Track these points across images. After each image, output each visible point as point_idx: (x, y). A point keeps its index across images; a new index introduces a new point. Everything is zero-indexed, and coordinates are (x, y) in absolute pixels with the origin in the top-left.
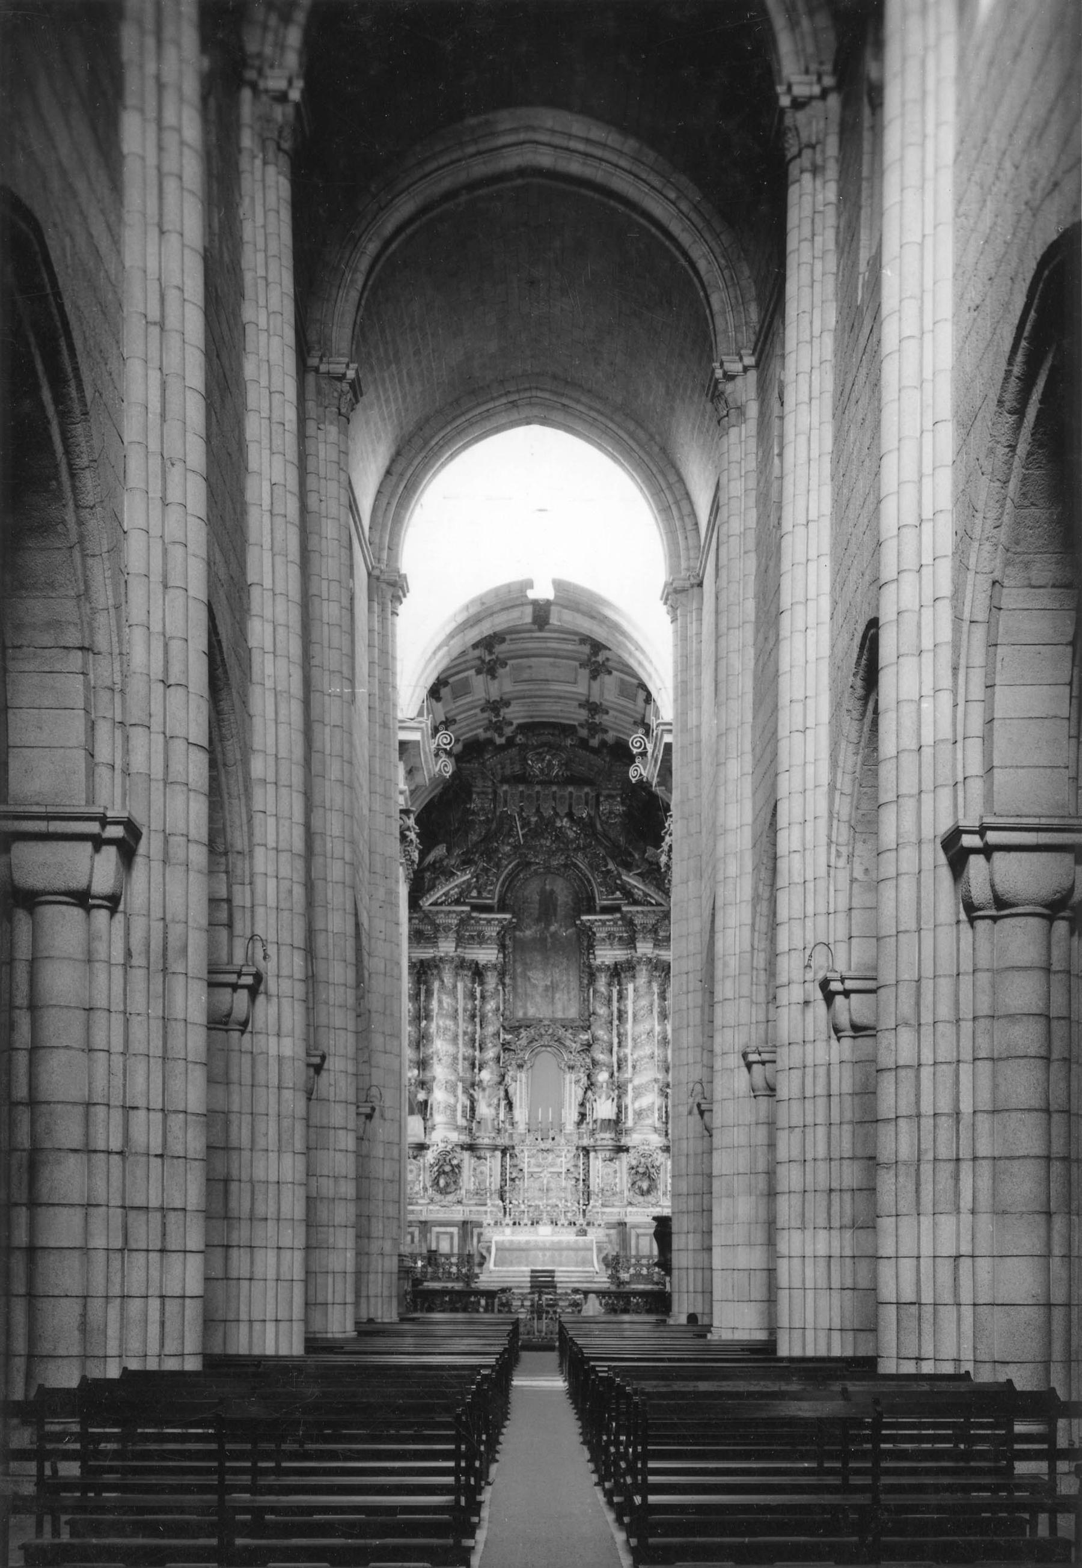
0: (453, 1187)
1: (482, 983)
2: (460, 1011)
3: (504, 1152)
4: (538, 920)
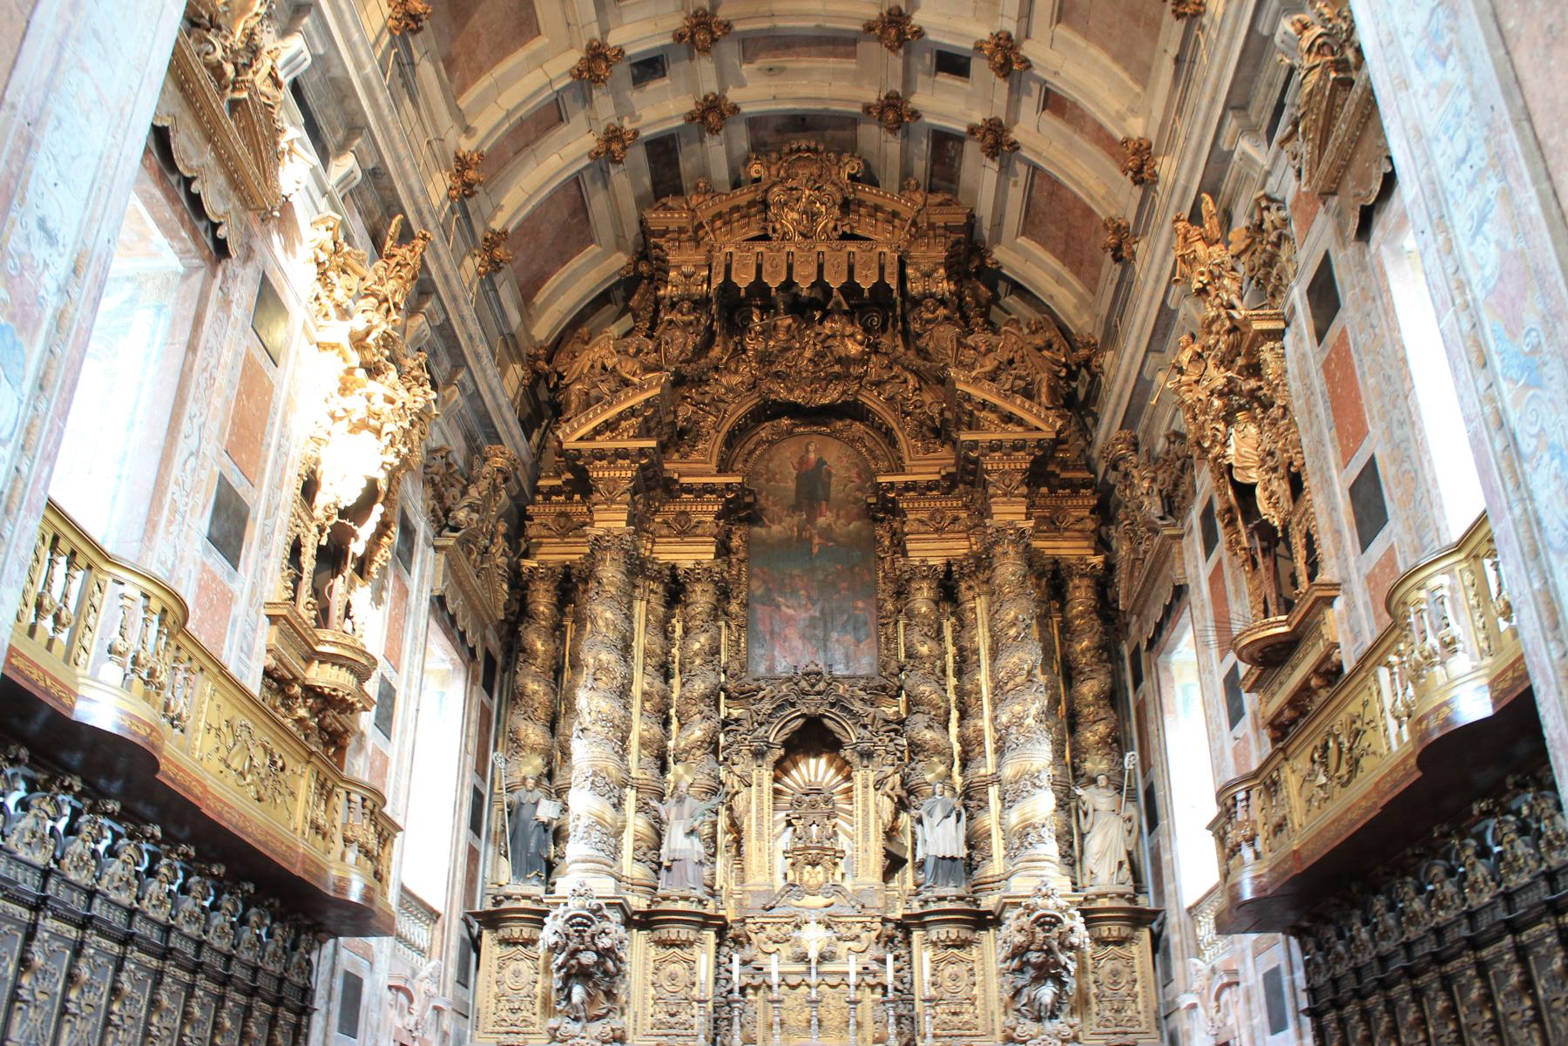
3: (722, 930)
4: (796, 508)
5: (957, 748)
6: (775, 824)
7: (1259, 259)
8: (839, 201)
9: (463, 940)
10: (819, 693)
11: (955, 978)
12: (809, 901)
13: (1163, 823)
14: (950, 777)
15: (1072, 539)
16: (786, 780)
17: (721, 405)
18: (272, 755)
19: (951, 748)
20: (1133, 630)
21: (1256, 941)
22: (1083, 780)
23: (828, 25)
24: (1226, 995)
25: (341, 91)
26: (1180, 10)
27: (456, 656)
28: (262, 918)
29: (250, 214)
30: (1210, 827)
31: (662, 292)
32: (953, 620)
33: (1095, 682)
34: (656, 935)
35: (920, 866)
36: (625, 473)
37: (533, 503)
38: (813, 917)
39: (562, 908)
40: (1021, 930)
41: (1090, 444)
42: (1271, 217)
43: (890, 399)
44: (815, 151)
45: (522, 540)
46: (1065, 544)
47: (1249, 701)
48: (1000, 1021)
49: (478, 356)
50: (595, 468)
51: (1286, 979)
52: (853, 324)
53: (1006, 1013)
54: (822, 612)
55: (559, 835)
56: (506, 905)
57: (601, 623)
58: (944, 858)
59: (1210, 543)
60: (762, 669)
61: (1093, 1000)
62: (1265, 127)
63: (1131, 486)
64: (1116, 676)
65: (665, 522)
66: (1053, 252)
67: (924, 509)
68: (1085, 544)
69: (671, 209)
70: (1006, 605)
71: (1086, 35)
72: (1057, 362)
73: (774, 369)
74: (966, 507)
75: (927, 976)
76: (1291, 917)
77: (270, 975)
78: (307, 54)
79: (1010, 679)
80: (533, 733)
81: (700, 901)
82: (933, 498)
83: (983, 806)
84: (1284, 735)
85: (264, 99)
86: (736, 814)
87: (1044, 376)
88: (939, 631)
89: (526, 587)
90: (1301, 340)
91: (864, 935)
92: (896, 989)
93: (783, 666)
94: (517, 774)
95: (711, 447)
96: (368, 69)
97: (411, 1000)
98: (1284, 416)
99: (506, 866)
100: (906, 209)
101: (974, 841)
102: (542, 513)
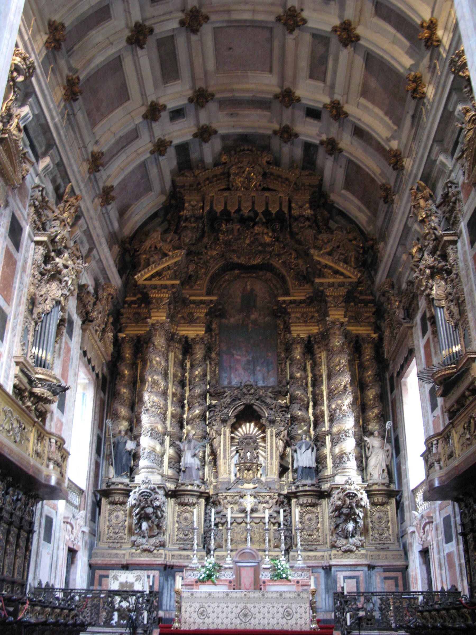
0: (156, 531)
2: (170, 376)
3: (208, 499)
5: (312, 418)
6: (231, 452)
7: (447, 209)
8: (262, 173)
9: (93, 502)
10: (251, 394)
11: (310, 520)
12: (246, 486)
13: (402, 452)
14: (309, 431)
15: (364, 326)
16: (237, 433)
17: (208, 264)
18: (20, 423)
19: (309, 419)
20: (391, 367)
21: (441, 504)
22: (367, 434)
23: (258, 95)
24: (427, 527)
25: (45, 129)
26: (415, 95)
27: (90, 377)
28: (14, 492)
29: (8, 187)
30: (422, 456)
31: (182, 213)
32: (311, 361)
33: (373, 390)
34: (179, 500)
35: (295, 471)
36: (166, 296)
37: (123, 308)
38: (249, 493)
39: (137, 489)
40: (339, 499)
41: (373, 282)
42: (453, 190)
43: (284, 263)
44: (251, 151)
45: (118, 324)
46: (362, 328)
47: (440, 401)
48: (329, 538)
49: (101, 244)
50: (151, 293)
51: (452, 520)
52: (267, 228)
53: (332, 535)
54: (253, 357)
55: (136, 456)
56: (112, 487)
57: (154, 362)
58: (306, 467)
59: (424, 331)
60: (226, 383)
61: (370, 530)
62: (450, 150)
63: (390, 303)
64: (383, 388)
65: (183, 317)
66: (357, 197)
67: (299, 312)
68: (370, 328)
69: (186, 176)
70: (335, 356)
71: (373, 102)
72: (358, 246)
73: (232, 248)
74: (317, 311)
75: (297, 519)
76: (455, 494)
77: (18, 516)
78: (31, 115)
79: (336, 389)
80: (123, 411)
81: (198, 486)
82: (303, 307)
83: (324, 445)
84: (454, 415)
85: (14, 137)
86: (214, 448)
87: (353, 253)
88: (305, 367)
89: (120, 346)
90: (464, 245)
91: (270, 501)
92: (284, 524)
93: (235, 382)
94: (117, 429)
95: (203, 283)
96: (57, 120)
97: (72, 528)
98: (456, 278)
99: (112, 470)
100: (292, 177)
101: (320, 460)
102: (127, 312)
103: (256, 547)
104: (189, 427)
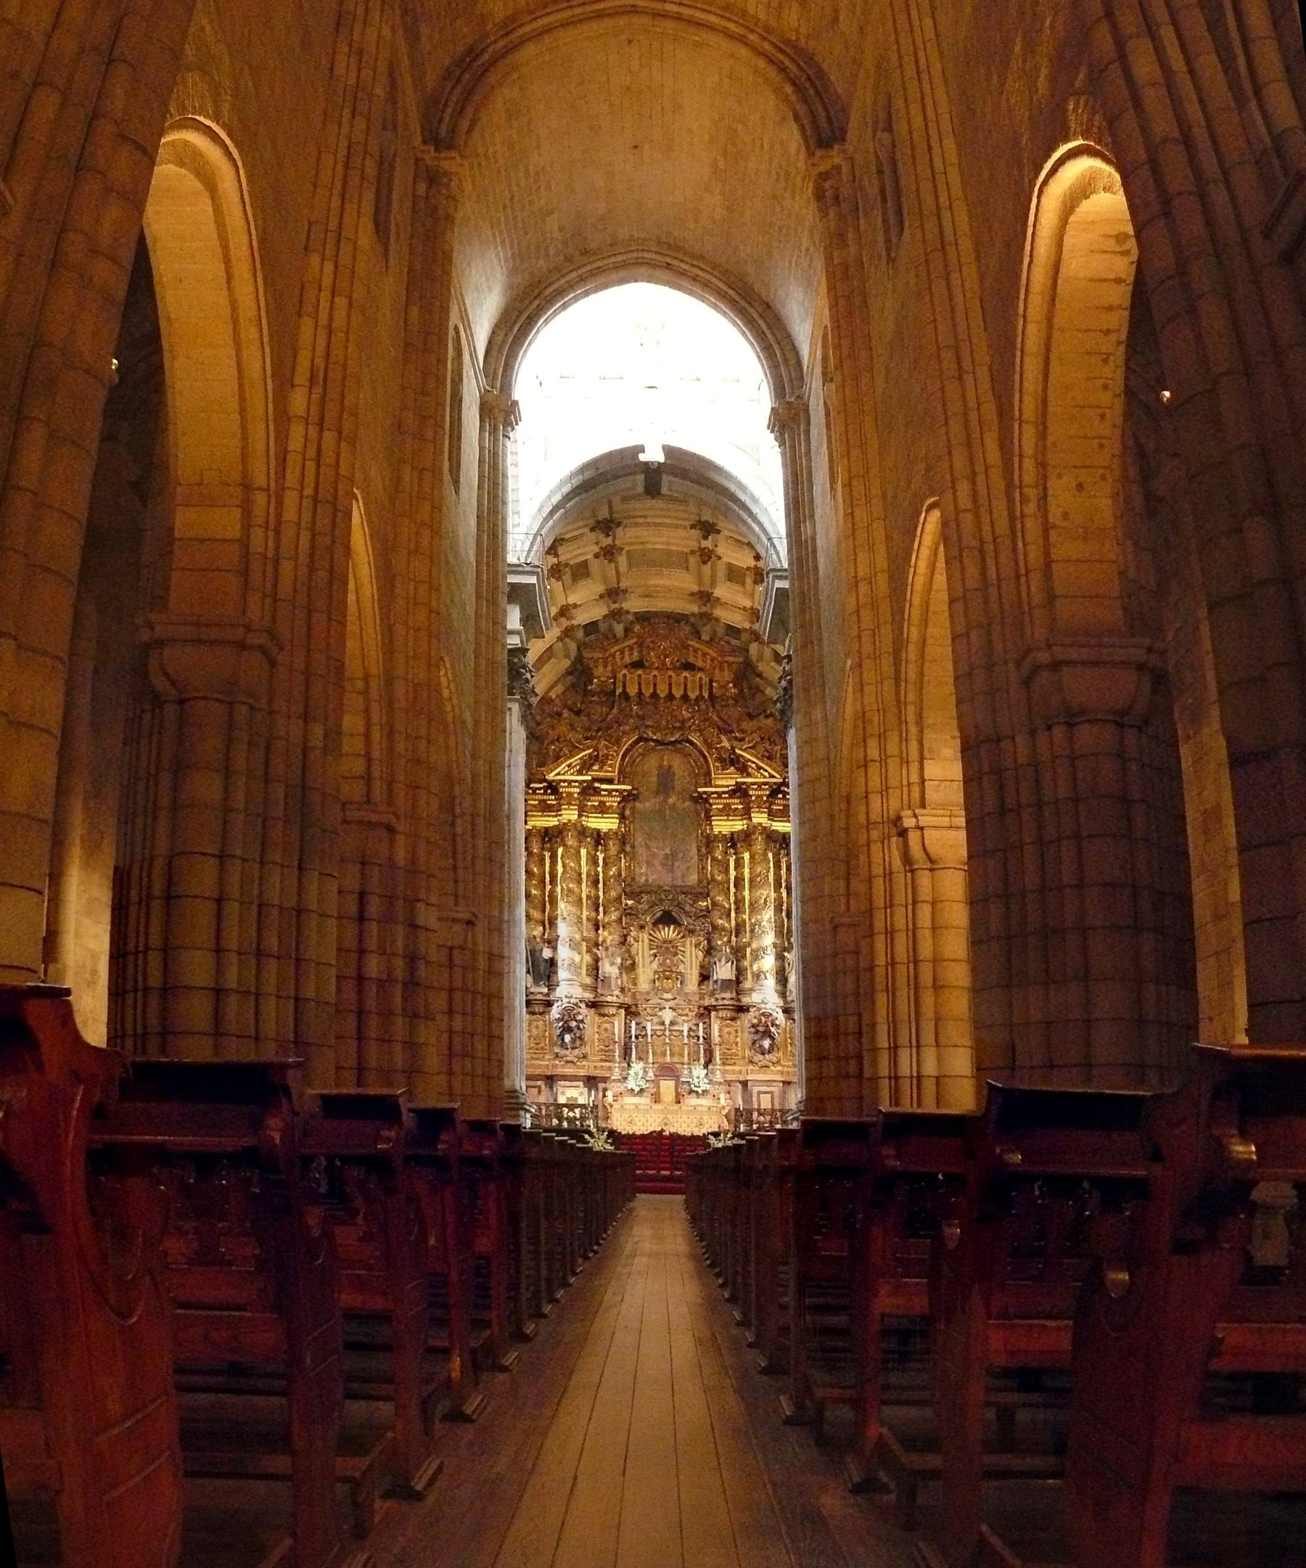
0: (578, 1043)
1: (605, 850)
2: (584, 876)
4: (658, 793)
39: (560, 1003)
43: (705, 741)
103: (676, 1059)
104: (606, 933)
